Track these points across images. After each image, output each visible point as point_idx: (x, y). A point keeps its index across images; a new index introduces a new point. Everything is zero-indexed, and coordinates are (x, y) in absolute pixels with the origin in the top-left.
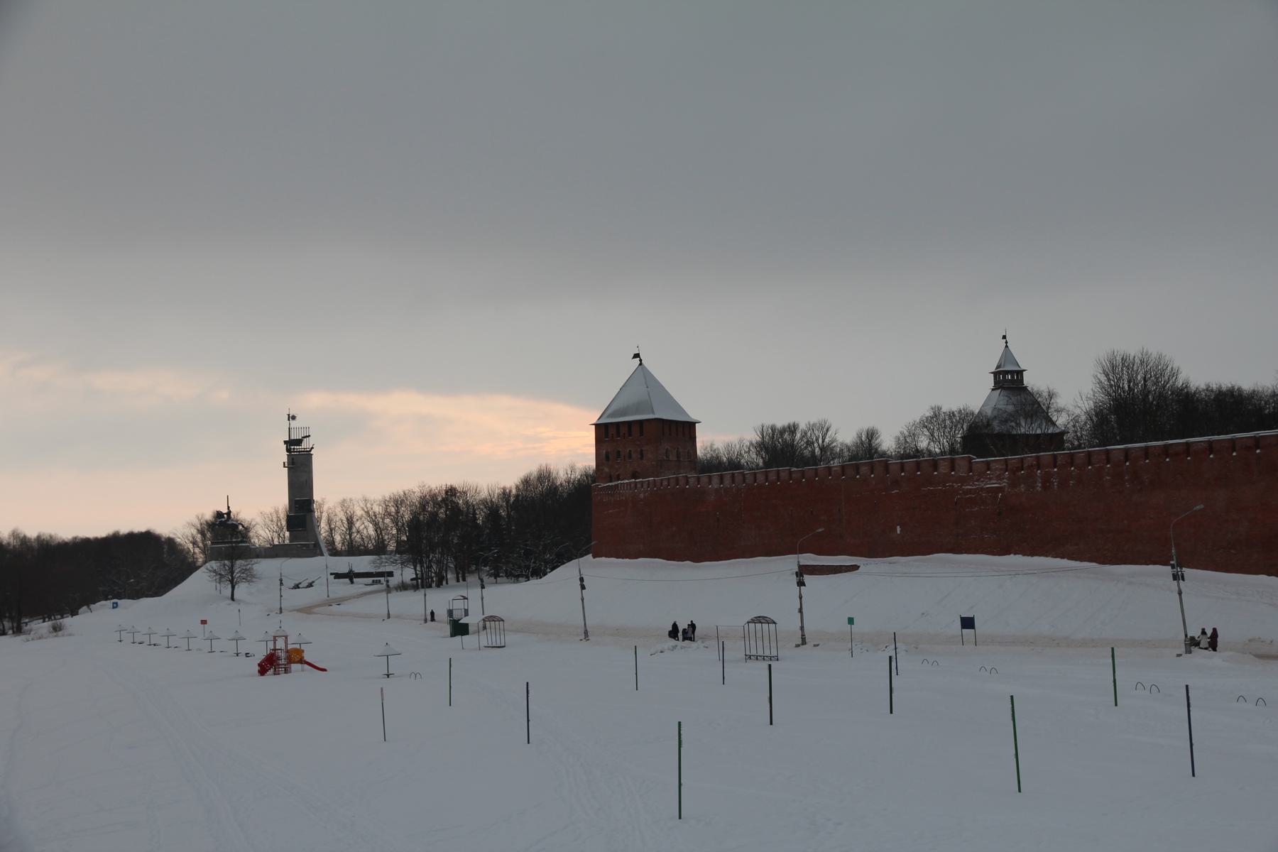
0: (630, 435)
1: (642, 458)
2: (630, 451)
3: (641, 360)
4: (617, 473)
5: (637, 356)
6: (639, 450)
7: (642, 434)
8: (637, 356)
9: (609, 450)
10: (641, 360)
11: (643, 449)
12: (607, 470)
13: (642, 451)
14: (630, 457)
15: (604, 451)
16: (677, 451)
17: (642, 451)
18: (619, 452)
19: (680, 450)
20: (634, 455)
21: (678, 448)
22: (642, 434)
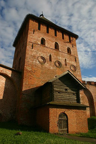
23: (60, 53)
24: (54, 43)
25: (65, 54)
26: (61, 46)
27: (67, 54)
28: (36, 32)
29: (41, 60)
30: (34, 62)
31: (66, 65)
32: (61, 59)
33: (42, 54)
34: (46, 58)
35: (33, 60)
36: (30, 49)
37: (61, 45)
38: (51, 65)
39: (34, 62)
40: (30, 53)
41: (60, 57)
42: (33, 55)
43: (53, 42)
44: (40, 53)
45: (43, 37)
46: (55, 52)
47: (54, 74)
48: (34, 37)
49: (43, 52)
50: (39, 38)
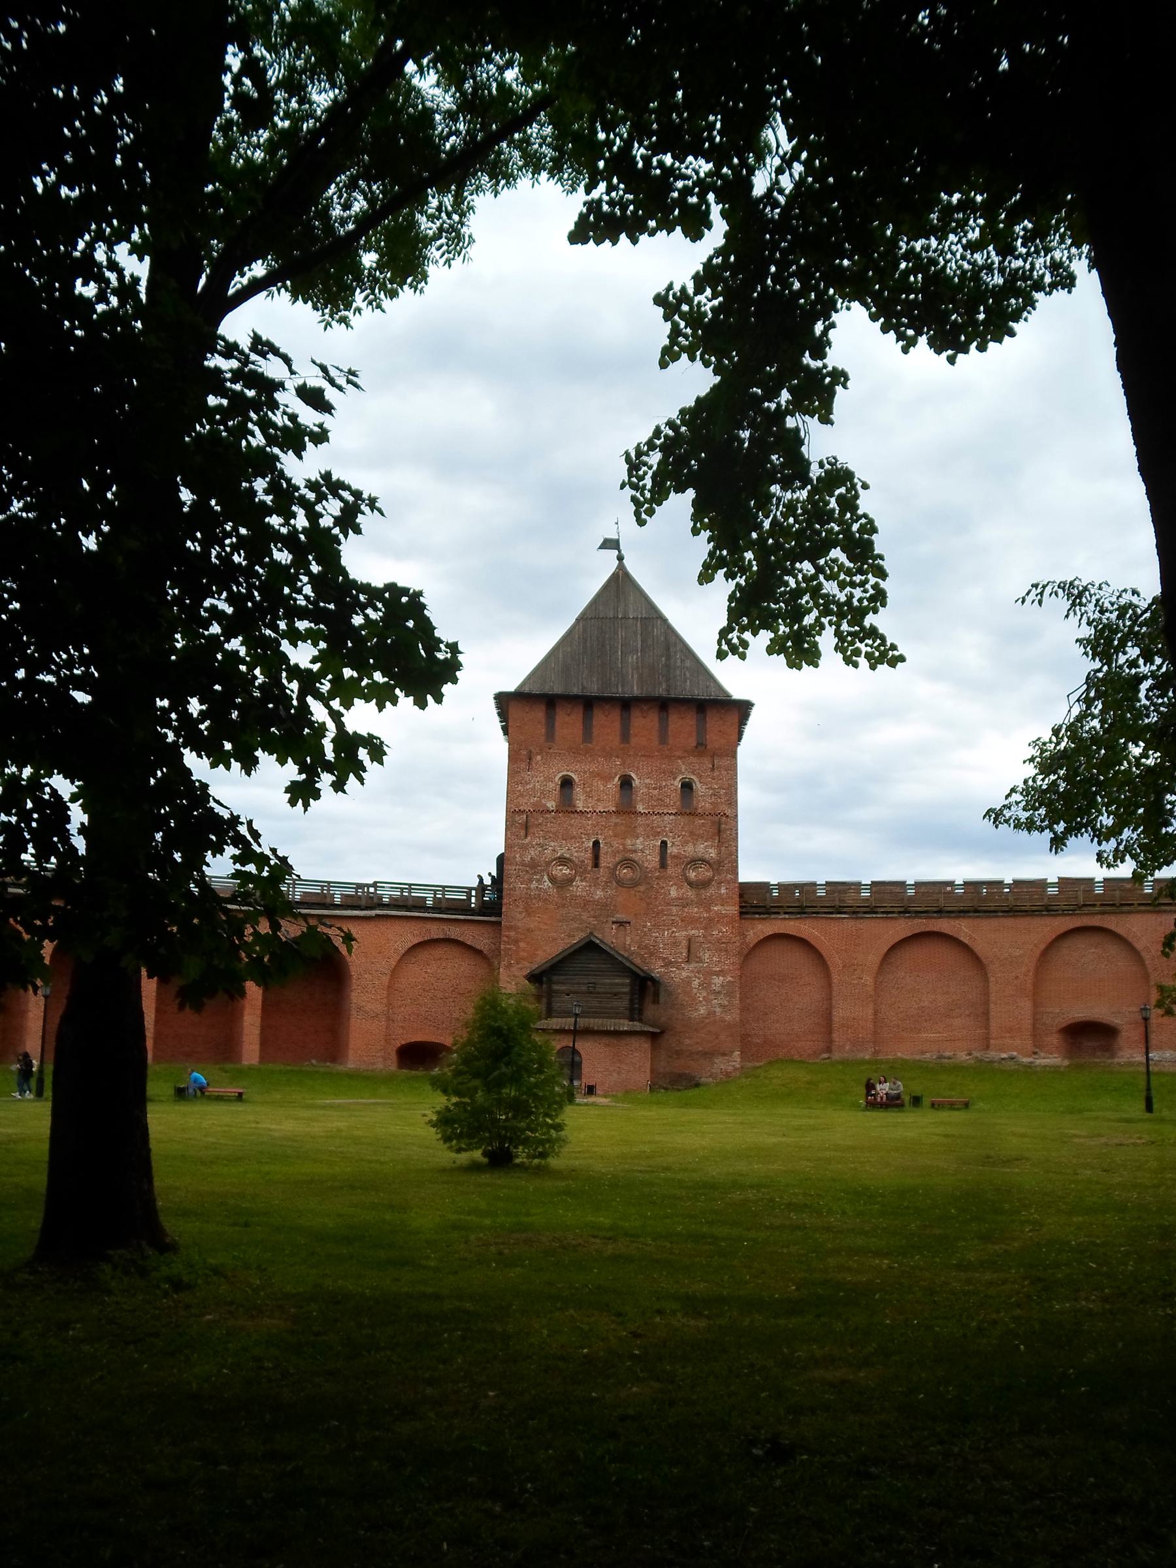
3: (620, 558)
5: (610, 544)
10: (620, 558)
24: (617, 779)
25: (666, 818)
26: (647, 786)
27: (672, 817)
28: (539, 758)
29: (561, 870)
30: (534, 885)
31: (663, 865)
32: (641, 847)
33: (560, 846)
34: (578, 857)
35: (531, 881)
36: (516, 841)
37: (647, 781)
38: (595, 883)
39: (532, 886)
40: (518, 856)
42: (527, 859)
43: (608, 778)
44: (552, 844)
45: (565, 773)
46: (616, 824)
47: (608, 916)
48: (528, 787)
49: (568, 837)
50: (549, 779)
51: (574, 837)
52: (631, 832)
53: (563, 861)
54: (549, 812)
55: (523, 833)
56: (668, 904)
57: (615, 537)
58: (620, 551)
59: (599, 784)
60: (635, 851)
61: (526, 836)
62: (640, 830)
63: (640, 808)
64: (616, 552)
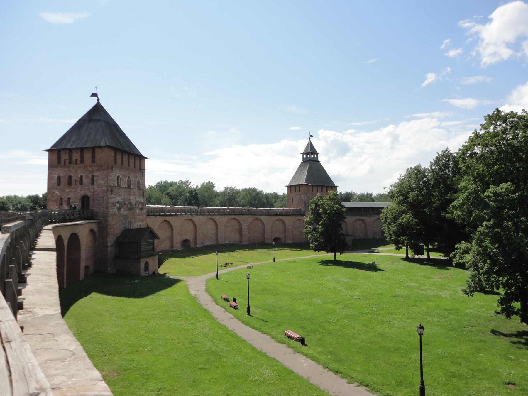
0: (82, 162)
1: (93, 183)
2: (81, 177)
3: (98, 100)
4: (68, 197)
5: (94, 95)
6: (90, 176)
7: (93, 161)
8: (94, 95)
9: (61, 175)
10: (98, 100)
11: (95, 174)
12: (57, 193)
13: (93, 177)
14: (81, 183)
15: (56, 176)
16: (128, 180)
17: (93, 177)
18: (70, 177)
19: (131, 179)
20: (85, 181)
21: (129, 177)
22: (93, 161)
23: (132, 191)
30: (114, 210)
41: (132, 197)
43: (126, 177)
44: (117, 197)
51: (121, 195)
52: (130, 194)
53: (118, 202)
54: (116, 186)
55: (111, 193)
56: (137, 215)
57: (96, 93)
58: (98, 97)
59: (124, 178)
60: (131, 200)
61: (112, 194)
62: (132, 193)
63: (132, 187)
64: (97, 98)
